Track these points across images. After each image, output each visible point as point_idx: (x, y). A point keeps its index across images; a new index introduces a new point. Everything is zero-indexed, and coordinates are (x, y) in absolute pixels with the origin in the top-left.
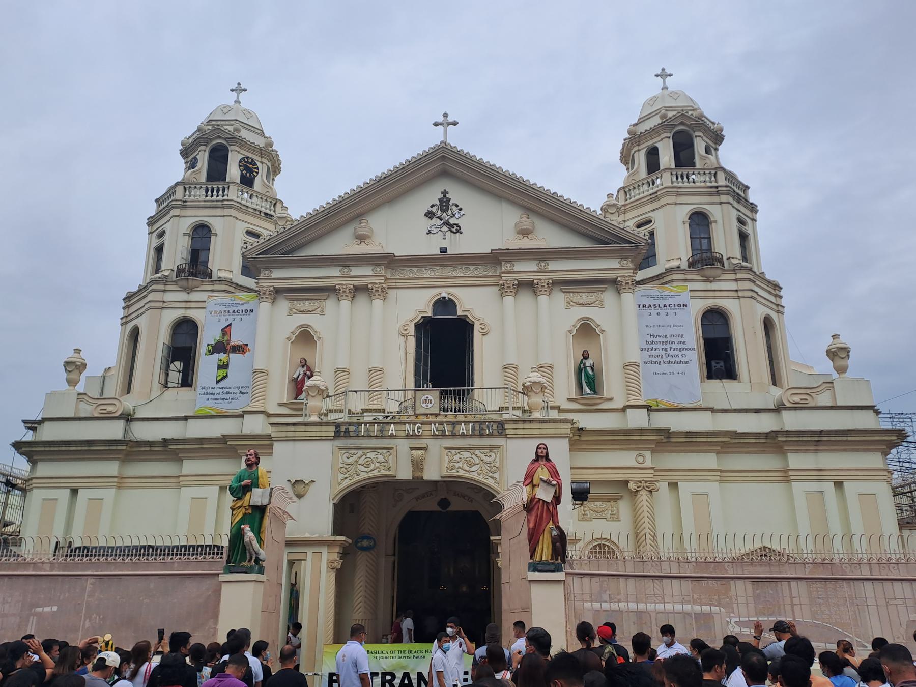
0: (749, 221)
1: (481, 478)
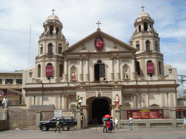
0: (158, 41)
1: (108, 97)
